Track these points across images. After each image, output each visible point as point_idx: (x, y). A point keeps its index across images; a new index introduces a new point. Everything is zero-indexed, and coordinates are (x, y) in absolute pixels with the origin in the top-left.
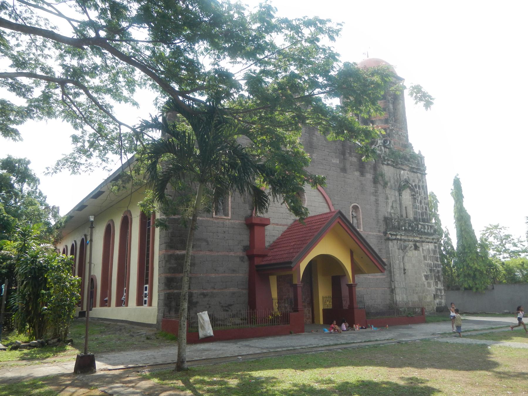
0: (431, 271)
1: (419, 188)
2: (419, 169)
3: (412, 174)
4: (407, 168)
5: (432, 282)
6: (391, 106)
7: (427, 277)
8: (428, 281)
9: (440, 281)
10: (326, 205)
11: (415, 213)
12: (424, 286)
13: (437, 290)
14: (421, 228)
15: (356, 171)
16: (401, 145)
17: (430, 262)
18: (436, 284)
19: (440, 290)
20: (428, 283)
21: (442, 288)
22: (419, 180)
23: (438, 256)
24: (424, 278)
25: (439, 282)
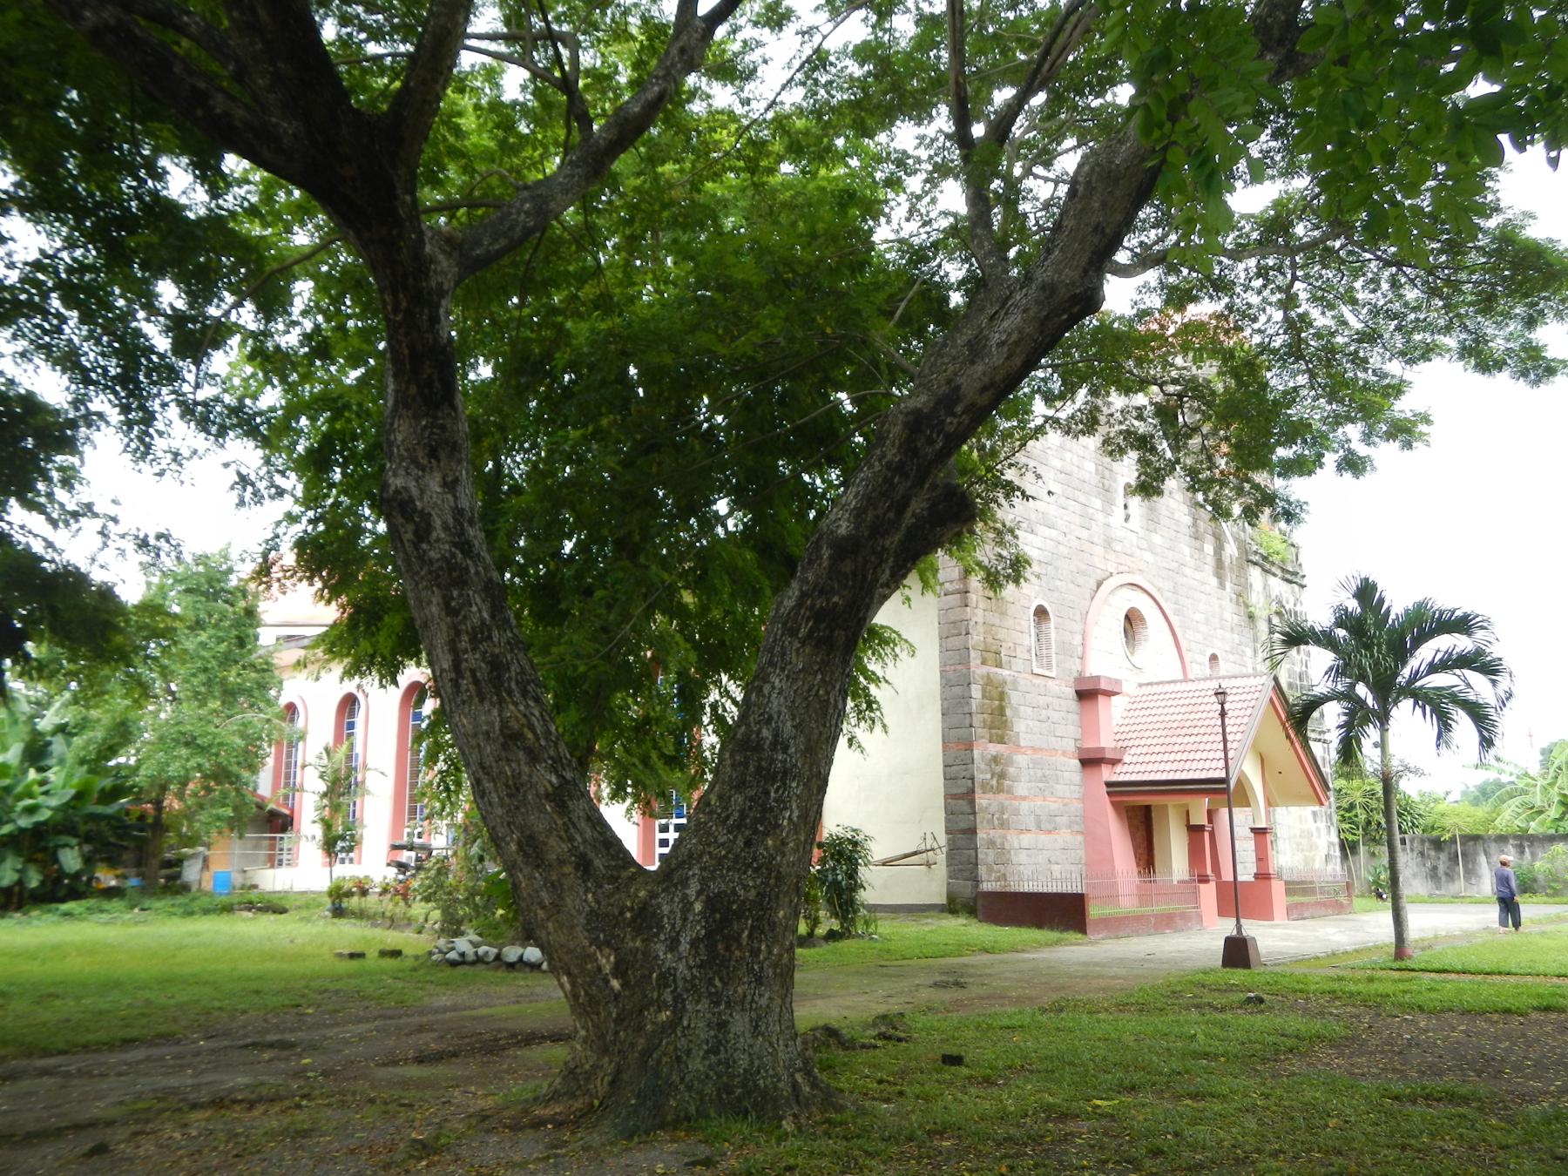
4: (1278, 572)
5: (1322, 825)
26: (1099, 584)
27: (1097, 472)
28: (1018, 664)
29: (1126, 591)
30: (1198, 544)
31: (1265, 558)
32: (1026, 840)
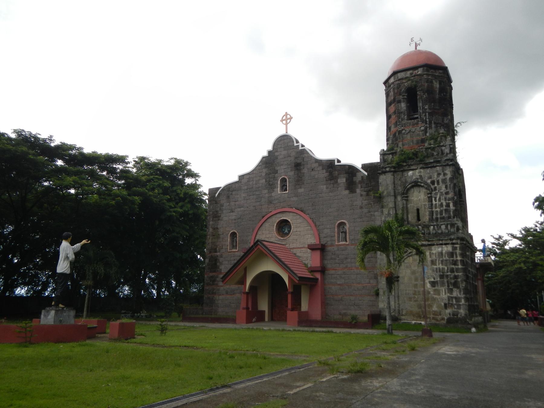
0: (442, 277)
1: (438, 183)
2: (439, 162)
3: (428, 171)
4: (421, 165)
6: (403, 105)
7: (433, 284)
8: (436, 288)
9: (458, 288)
10: (310, 227)
11: (432, 213)
12: (429, 293)
13: (450, 298)
14: (434, 228)
15: (346, 189)
16: (415, 142)
17: (441, 266)
18: (451, 291)
19: (458, 299)
20: (435, 290)
21: (463, 296)
22: (439, 174)
23: (459, 258)
24: (428, 285)
25: (455, 289)
26: (263, 217)
27: (266, 181)
28: (223, 250)
29: (278, 215)
30: (332, 182)
31: (394, 167)
32: (221, 297)
